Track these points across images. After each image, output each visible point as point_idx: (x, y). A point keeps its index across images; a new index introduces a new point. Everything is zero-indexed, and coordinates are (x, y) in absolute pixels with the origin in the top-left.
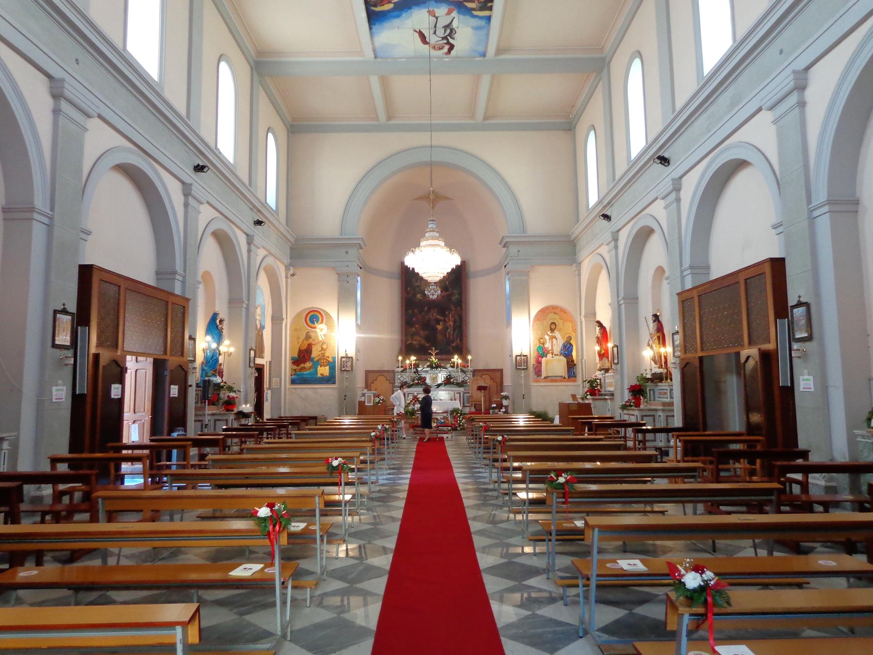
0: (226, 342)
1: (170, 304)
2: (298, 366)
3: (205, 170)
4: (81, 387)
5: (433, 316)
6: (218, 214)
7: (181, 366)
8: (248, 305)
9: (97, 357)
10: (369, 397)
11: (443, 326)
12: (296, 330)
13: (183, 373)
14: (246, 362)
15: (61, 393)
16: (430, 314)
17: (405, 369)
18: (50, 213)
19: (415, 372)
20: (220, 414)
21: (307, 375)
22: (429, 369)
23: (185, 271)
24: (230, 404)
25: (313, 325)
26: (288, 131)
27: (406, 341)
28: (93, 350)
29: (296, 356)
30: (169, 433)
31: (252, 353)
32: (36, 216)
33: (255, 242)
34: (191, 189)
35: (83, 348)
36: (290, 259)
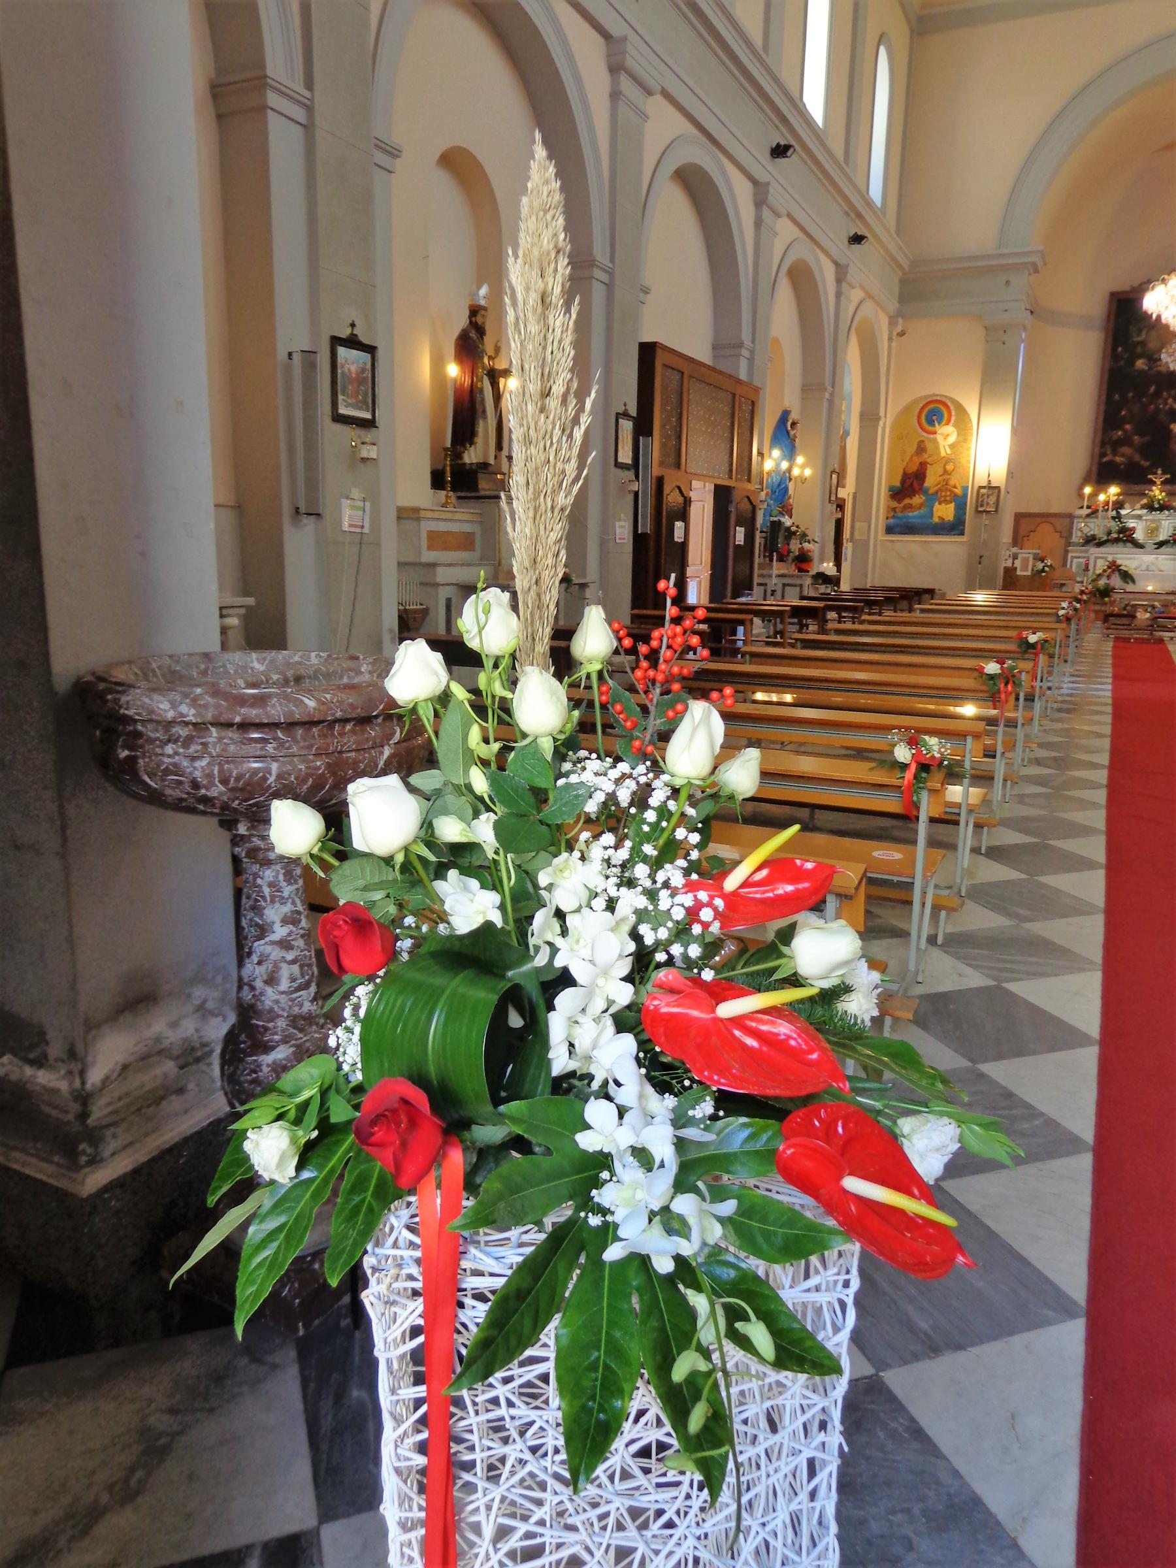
0: (800, 460)
1: (737, 397)
2: (899, 501)
3: (789, 154)
4: (644, 525)
6: (800, 234)
7: (748, 498)
8: (832, 394)
9: (660, 481)
10: (1026, 561)
12: (900, 437)
13: (749, 507)
14: (824, 492)
15: (623, 531)
16: (1161, 401)
17: (1095, 512)
18: (610, 265)
19: (1113, 518)
20: (792, 576)
21: (914, 517)
22: (1145, 511)
23: (753, 342)
24: (803, 559)
25: (930, 428)
26: (912, 31)
27: (1103, 455)
28: (656, 471)
29: (898, 484)
30: (736, 595)
31: (834, 476)
32: (597, 273)
33: (849, 277)
34: (768, 192)
35: (645, 467)
36: (899, 302)
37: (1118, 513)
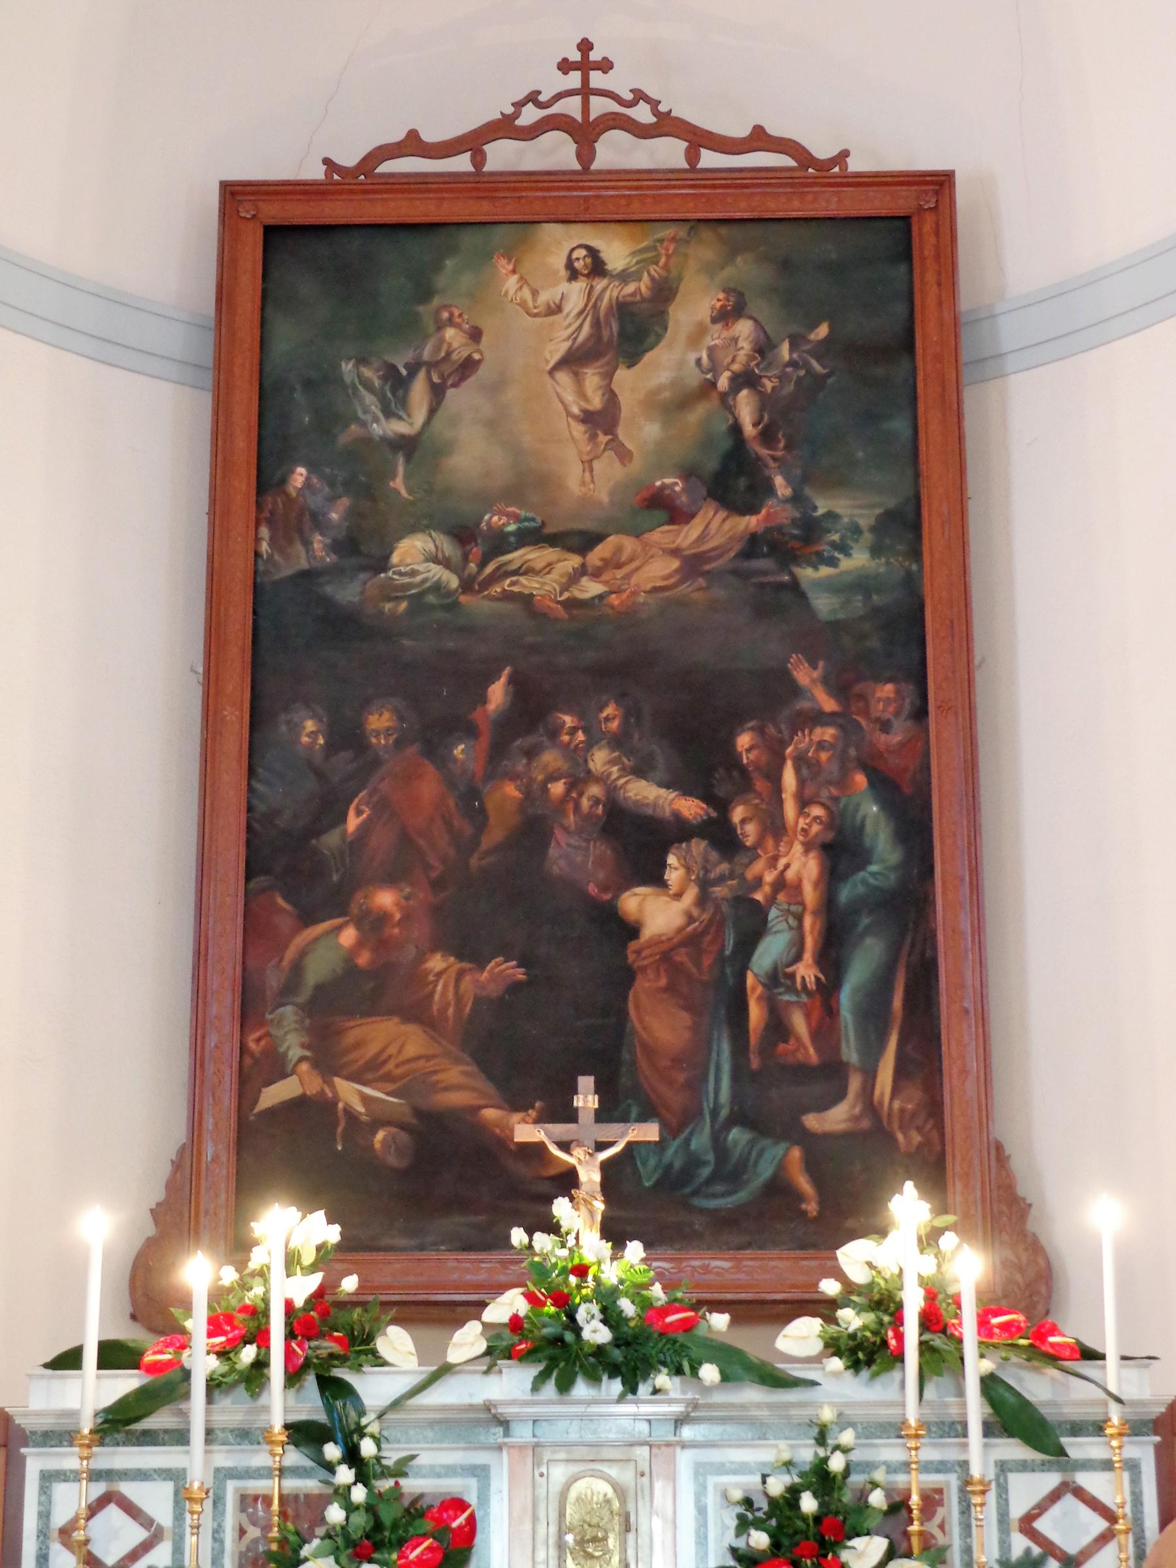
5: (578, 780)
11: (703, 900)
16: (551, 758)
37: (333, 1389)
